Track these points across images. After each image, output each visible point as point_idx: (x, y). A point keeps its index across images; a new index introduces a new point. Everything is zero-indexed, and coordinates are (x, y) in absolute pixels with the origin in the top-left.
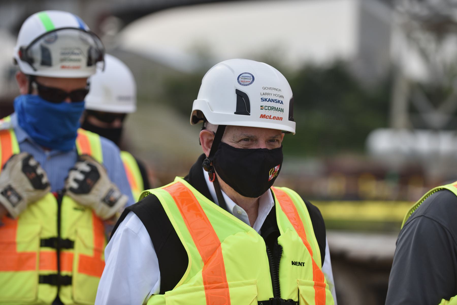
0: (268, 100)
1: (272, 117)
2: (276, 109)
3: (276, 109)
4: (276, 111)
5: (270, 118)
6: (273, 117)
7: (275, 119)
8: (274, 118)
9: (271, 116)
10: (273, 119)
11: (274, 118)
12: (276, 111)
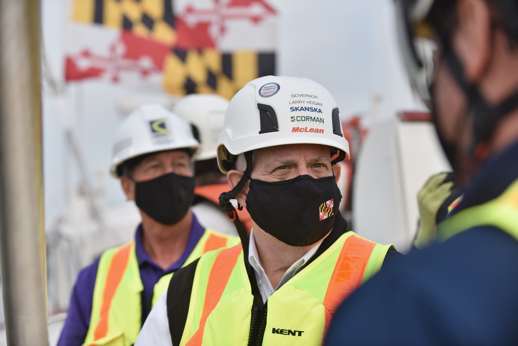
0: (299, 109)
1: (308, 130)
2: (313, 119)
3: (313, 119)
4: (313, 121)
5: (306, 131)
6: (310, 130)
7: (313, 132)
8: (312, 131)
9: (306, 128)
10: (310, 131)
11: (311, 130)
12: (313, 121)
